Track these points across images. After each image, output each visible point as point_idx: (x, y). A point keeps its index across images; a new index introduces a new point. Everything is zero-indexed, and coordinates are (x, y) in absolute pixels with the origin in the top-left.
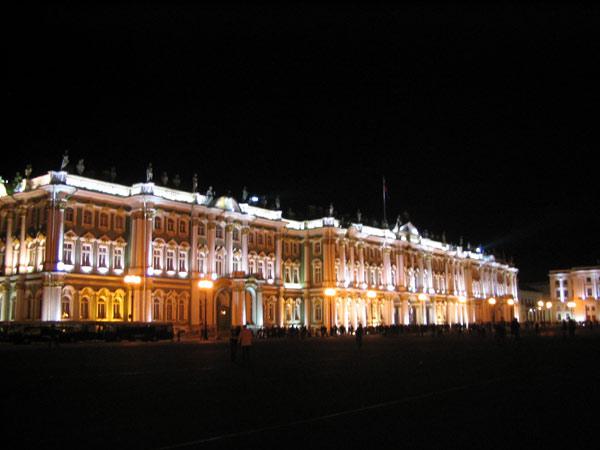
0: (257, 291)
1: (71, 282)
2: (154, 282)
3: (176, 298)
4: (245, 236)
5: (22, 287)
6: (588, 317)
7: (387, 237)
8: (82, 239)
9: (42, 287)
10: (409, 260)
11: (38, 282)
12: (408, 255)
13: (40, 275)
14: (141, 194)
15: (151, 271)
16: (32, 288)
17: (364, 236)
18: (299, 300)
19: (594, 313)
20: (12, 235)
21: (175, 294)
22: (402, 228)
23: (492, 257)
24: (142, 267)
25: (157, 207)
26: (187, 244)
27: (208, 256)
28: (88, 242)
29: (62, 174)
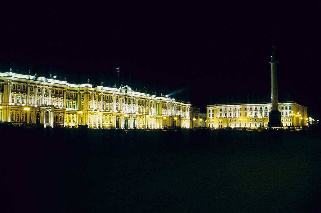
0: (51, 111)
2: (11, 107)
6: (219, 125)
7: (114, 91)
10: (126, 100)
14: (7, 76)
15: (10, 104)
17: (104, 91)
18: (75, 115)
21: (20, 112)
22: (123, 88)
23: (174, 99)
24: (7, 102)
25: (13, 81)
26: (25, 94)
27: (34, 98)
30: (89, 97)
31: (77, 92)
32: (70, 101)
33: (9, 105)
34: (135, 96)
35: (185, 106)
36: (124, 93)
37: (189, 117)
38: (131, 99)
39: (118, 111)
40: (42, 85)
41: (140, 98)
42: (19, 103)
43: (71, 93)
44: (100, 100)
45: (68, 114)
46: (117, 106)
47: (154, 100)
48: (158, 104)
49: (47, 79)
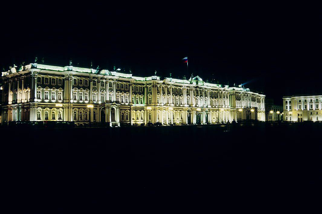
2: (73, 105)
3: (84, 111)
4: (115, 85)
5: (23, 108)
6: (299, 119)
7: (184, 83)
8: (44, 89)
9: (29, 108)
10: (197, 93)
11: (28, 106)
12: (197, 90)
13: (28, 104)
14: (67, 71)
15: (72, 101)
16: (26, 109)
17: (173, 83)
20: (19, 88)
21: (83, 110)
22: (193, 79)
23: (248, 89)
25: (74, 76)
27: (97, 94)
28: (47, 90)
29: (35, 64)
30: (157, 91)
31: (144, 86)
32: (136, 96)
33: (70, 103)
34: (207, 87)
36: (194, 84)
37: (264, 109)
38: (203, 91)
39: (188, 106)
40: (106, 79)
41: (212, 90)
43: (137, 87)
44: (170, 93)
45: (135, 110)
46: (188, 99)
47: (227, 91)
48: (232, 95)
49: (111, 72)
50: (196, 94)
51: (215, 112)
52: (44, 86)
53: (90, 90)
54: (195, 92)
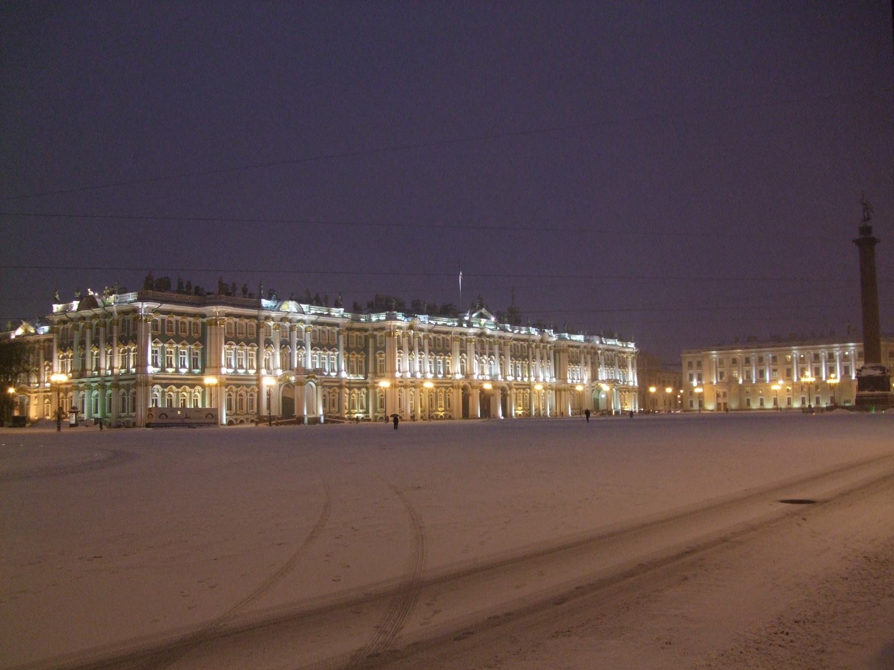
0: (317, 385)
1: (158, 381)
3: (247, 392)
6: (719, 404)
8: (166, 345)
11: (132, 382)
12: (482, 341)
13: (133, 377)
15: (224, 370)
19: (726, 401)
22: (474, 315)
31: (367, 334)
35: (624, 353)
42: (241, 367)
46: (462, 362)
48: (559, 352)
50: (479, 350)
51: (522, 391)
52: (164, 339)
53: (258, 345)
54: (479, 347)
